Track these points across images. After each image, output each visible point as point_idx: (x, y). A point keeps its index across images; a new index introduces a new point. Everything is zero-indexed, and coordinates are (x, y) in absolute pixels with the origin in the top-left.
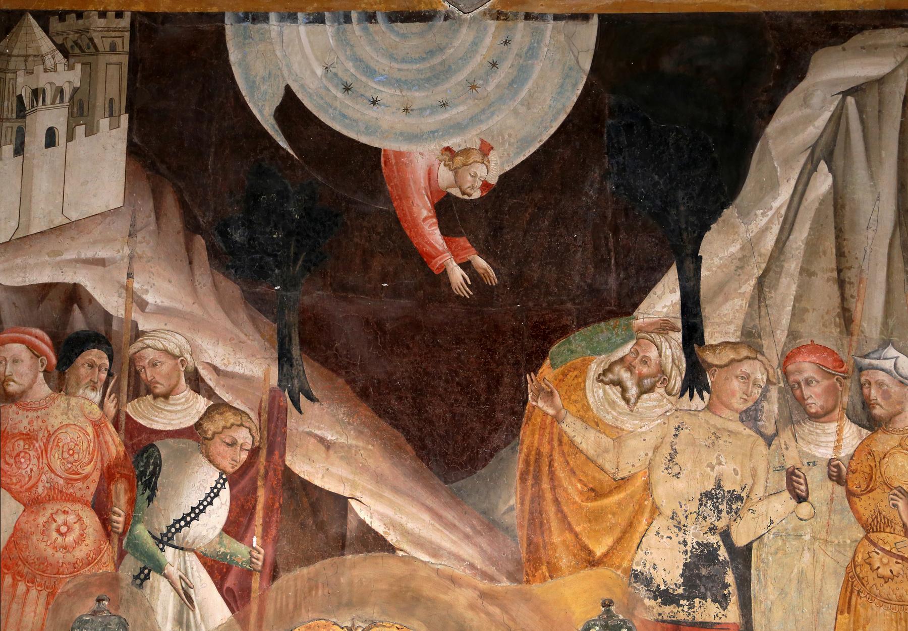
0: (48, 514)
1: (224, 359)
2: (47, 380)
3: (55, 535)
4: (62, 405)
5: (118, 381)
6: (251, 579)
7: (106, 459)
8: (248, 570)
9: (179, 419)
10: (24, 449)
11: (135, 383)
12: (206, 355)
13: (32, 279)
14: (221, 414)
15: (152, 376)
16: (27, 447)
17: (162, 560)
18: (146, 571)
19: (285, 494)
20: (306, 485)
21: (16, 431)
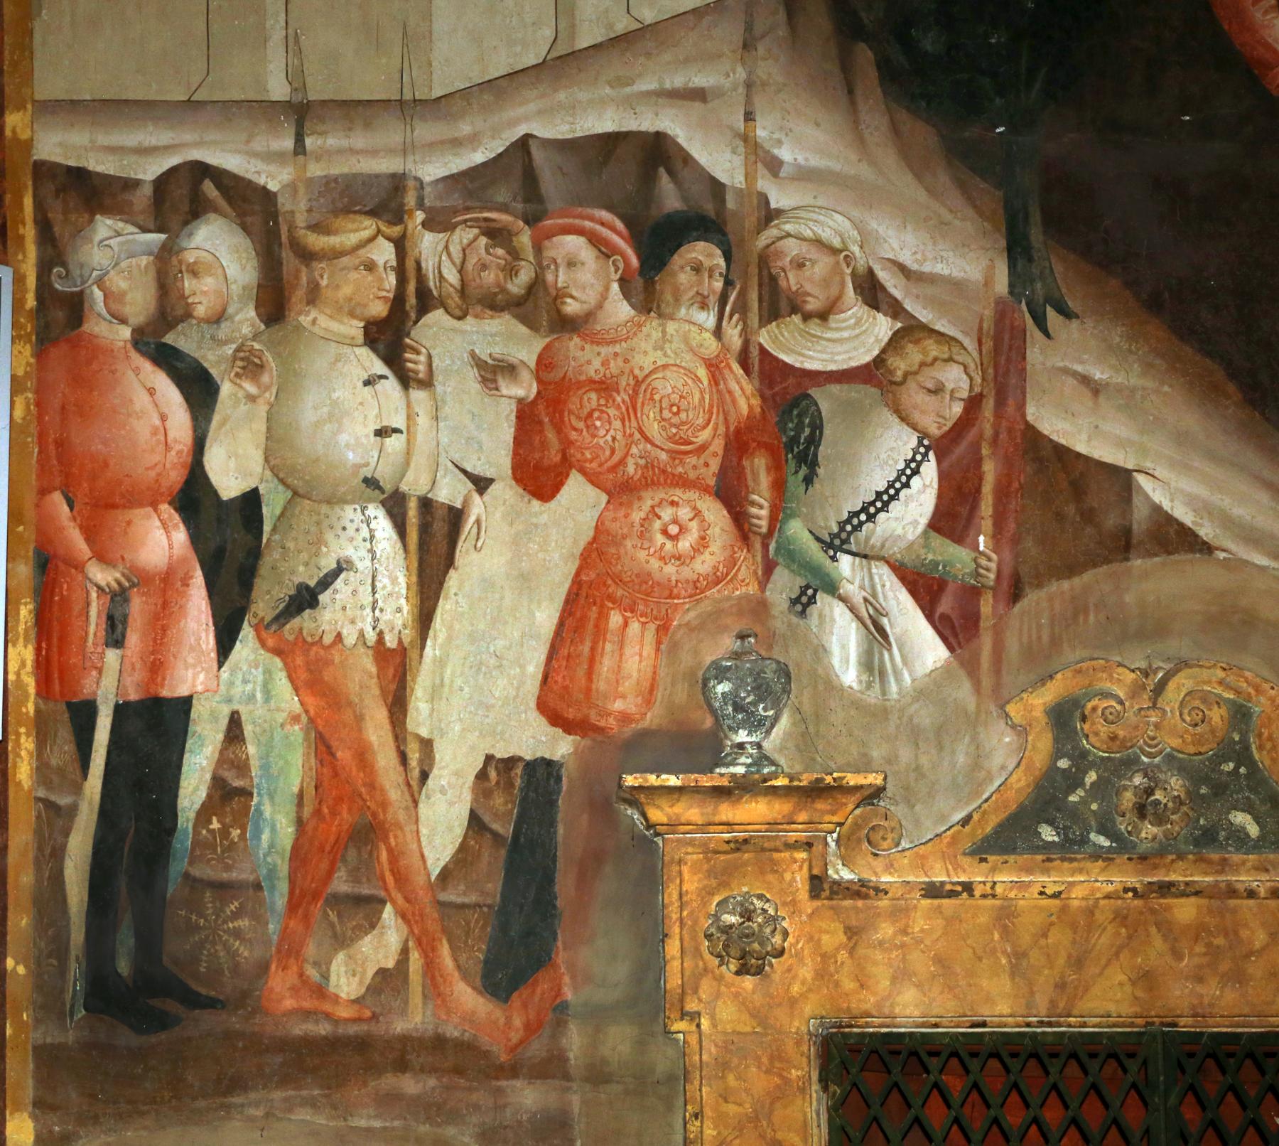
1: (915, 253)
2: (626, 293)
3: (660, 539)
5: (743, 294)
6: (979, 601)
7: (732, 419)
8: (973, 587)
9: (847, 352)
10: (599, 405)
14: (917, 342)
16: (602, 402)
17: (834, 575)
18: (810, 592)
19: (1028, 468)
20: (1063, 453)
21: (583, 378)
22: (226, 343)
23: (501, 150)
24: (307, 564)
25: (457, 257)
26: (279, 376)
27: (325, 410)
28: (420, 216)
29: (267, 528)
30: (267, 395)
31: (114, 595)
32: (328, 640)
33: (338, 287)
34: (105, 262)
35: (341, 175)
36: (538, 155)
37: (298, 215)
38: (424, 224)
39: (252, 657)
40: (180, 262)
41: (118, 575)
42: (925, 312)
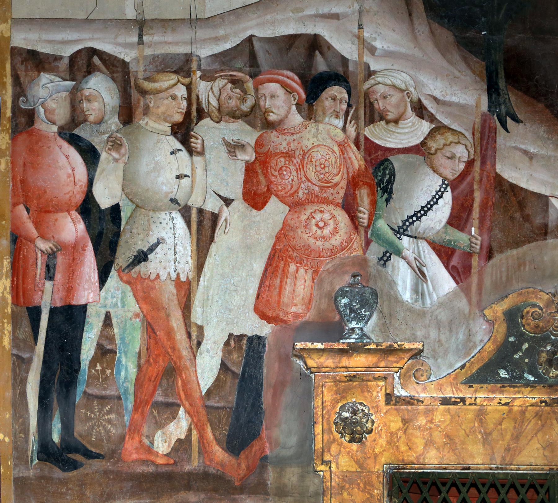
0: (308, 212)
1: (442, 91)
3: (315, 228)
4: (313, 130)
5: (357, 110)
6: (471, 259)
7: (351, 170)
8: (469, 253)
10: (285, 164)
11: (370, 112)
12: (427, 88)
13: (280, 31)
14: (442, 134)
15: (384, 106)
16: (287, 162)
17: (400, 246)
18: (388, 255)
19: (497, 195)
20: (514, 188)
21: (278, 151)
22: (103, 133)
23: (238, 43)
24: (142, 240)
25: (217, 92)
26: (129, 150)
27: (152, 166)
28: (199, 74)
29: (123, 223)
30: (124, 158)
31: (49, 255)
32: (153, 277)
33: (158, 107)
34: (45, 95)
35: (161, 54)
36: (257, 45)
37: (139, 73)
38: (200, 77)
39: (116, 285)
40: (82, 95)
41: (51, 245)
42: (446, 120)
